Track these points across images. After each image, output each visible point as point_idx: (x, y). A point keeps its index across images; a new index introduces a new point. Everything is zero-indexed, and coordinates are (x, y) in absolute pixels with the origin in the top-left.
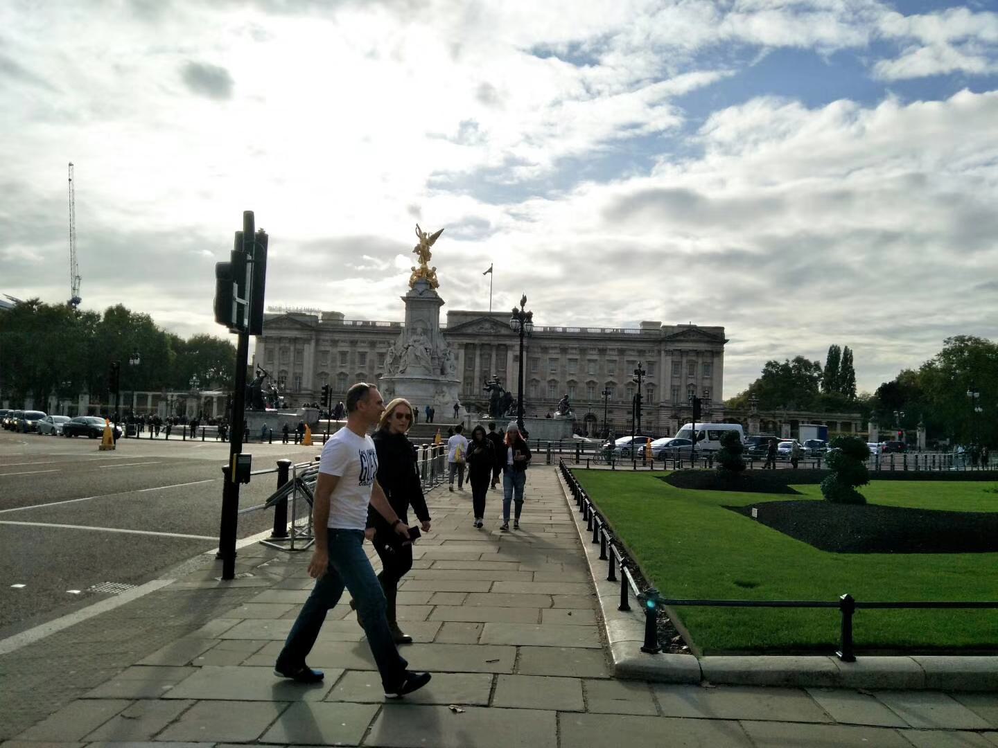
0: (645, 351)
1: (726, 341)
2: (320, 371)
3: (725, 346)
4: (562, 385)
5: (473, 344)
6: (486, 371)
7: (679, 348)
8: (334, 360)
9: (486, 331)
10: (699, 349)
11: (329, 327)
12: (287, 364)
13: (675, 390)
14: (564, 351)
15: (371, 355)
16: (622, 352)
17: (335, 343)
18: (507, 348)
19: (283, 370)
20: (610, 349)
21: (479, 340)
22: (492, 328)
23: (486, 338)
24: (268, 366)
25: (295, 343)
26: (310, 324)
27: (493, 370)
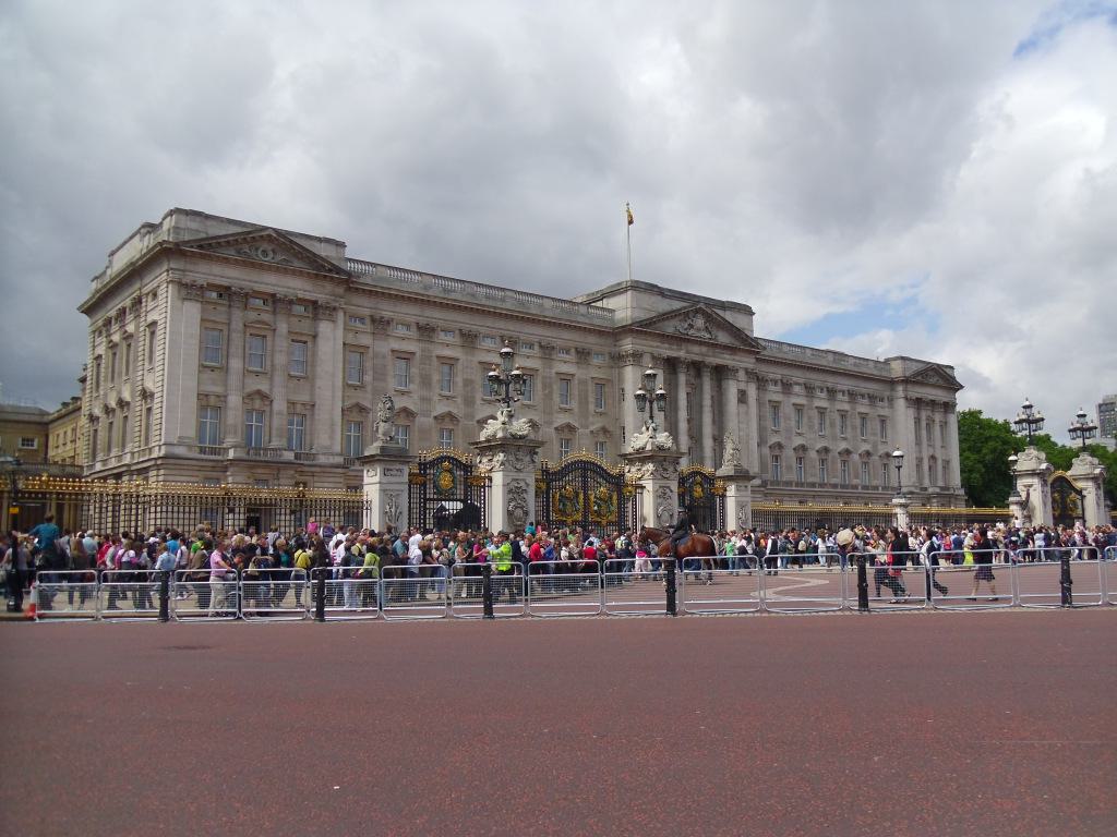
3: (957, 395)
4: (789, 454)
7: (919, 396)
8: (380, 375)
9: (699, 335)
11: (369, 282)
12: (268, 374)
14: (787, 387)
15: (468, 364)
16: (852, 395)
17: (380, 325)
19: (259, 392)
21: (688, 352)
23: (696, 349)
24: (208, 375)
25: (290, 314)
27: (707, 418)
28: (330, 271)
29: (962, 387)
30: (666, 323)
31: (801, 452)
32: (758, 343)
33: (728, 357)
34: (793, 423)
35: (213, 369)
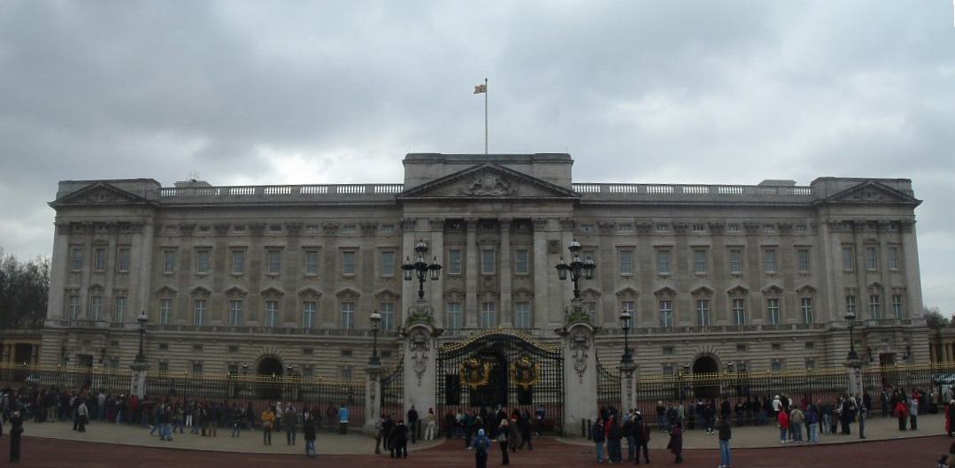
0: (790, 227)
1: (918, 203)
2: (162, 286)
5: (461, 221)
6: (488, 278)
7: (849, 218)
8: (186, 265)
9: (488, 193)
10: (880, 219)
13: (851, 298)
14: (644, 230)
16: (751, 229)
17: (187, 230)
18: (527, 226)
20: (731, 225)
22: (499, 185)
23: (487, 207)
26: (142, 195)
27: (506, 276)
28: (136, 200)
29: (921, 201)
30: (447, 188)
31: (666, 296)
32: (570, 192)
33: (532, 209)
34: (654, 266)
35: (76, 273)
